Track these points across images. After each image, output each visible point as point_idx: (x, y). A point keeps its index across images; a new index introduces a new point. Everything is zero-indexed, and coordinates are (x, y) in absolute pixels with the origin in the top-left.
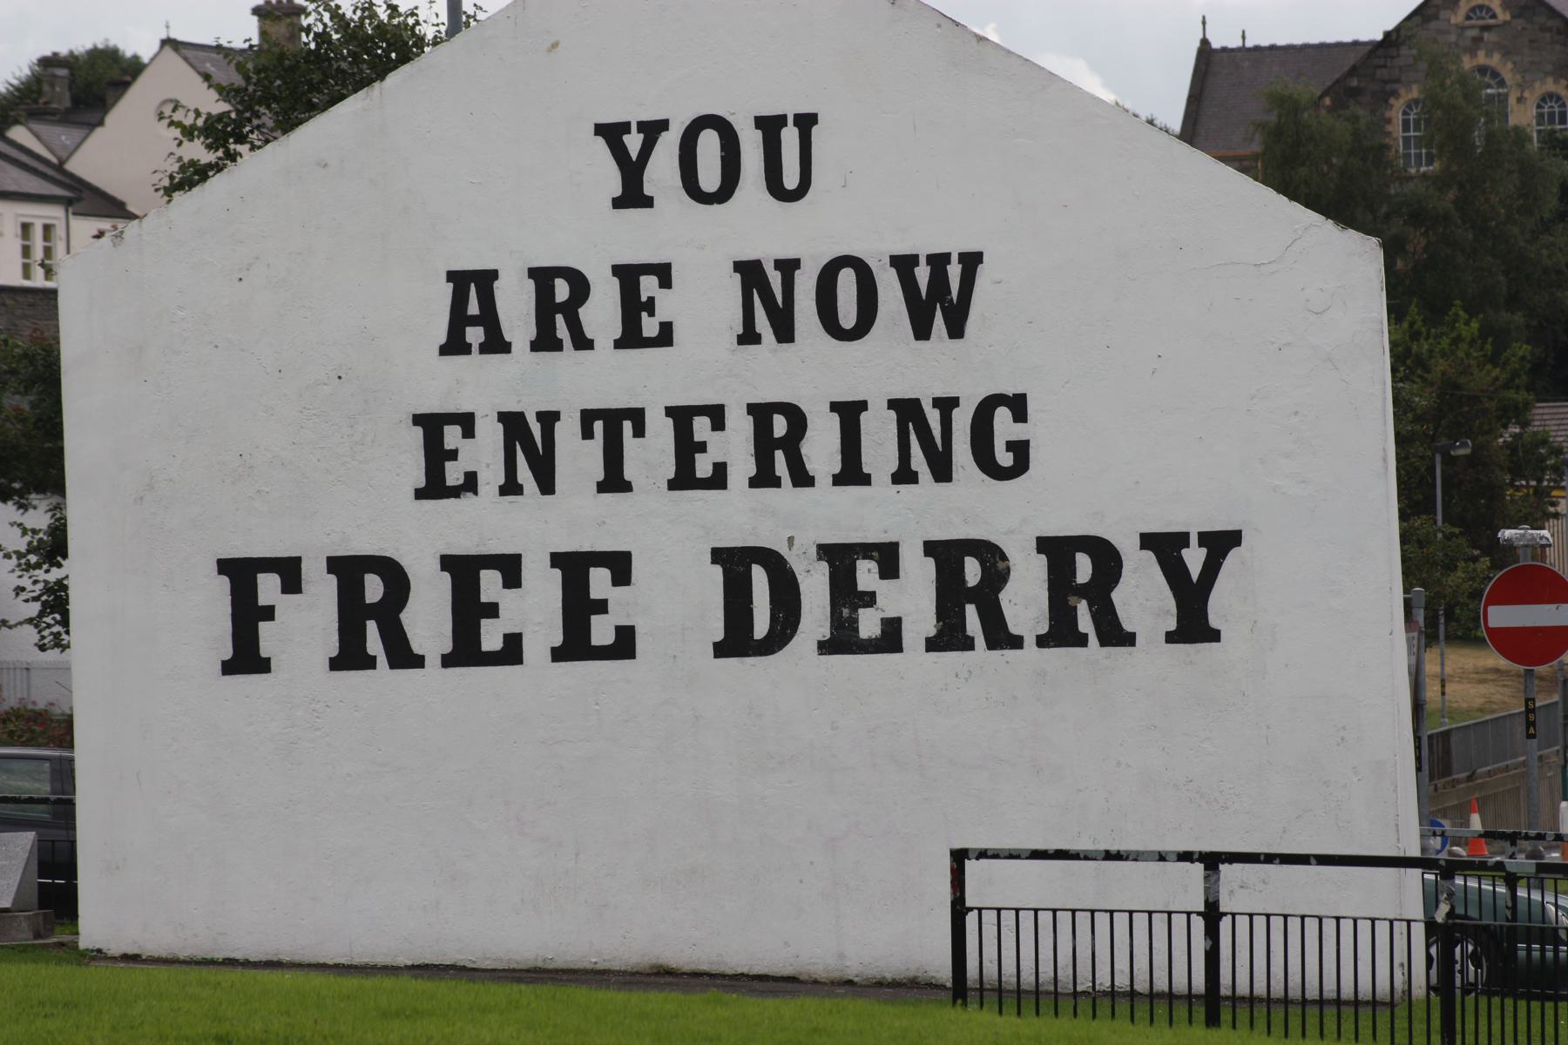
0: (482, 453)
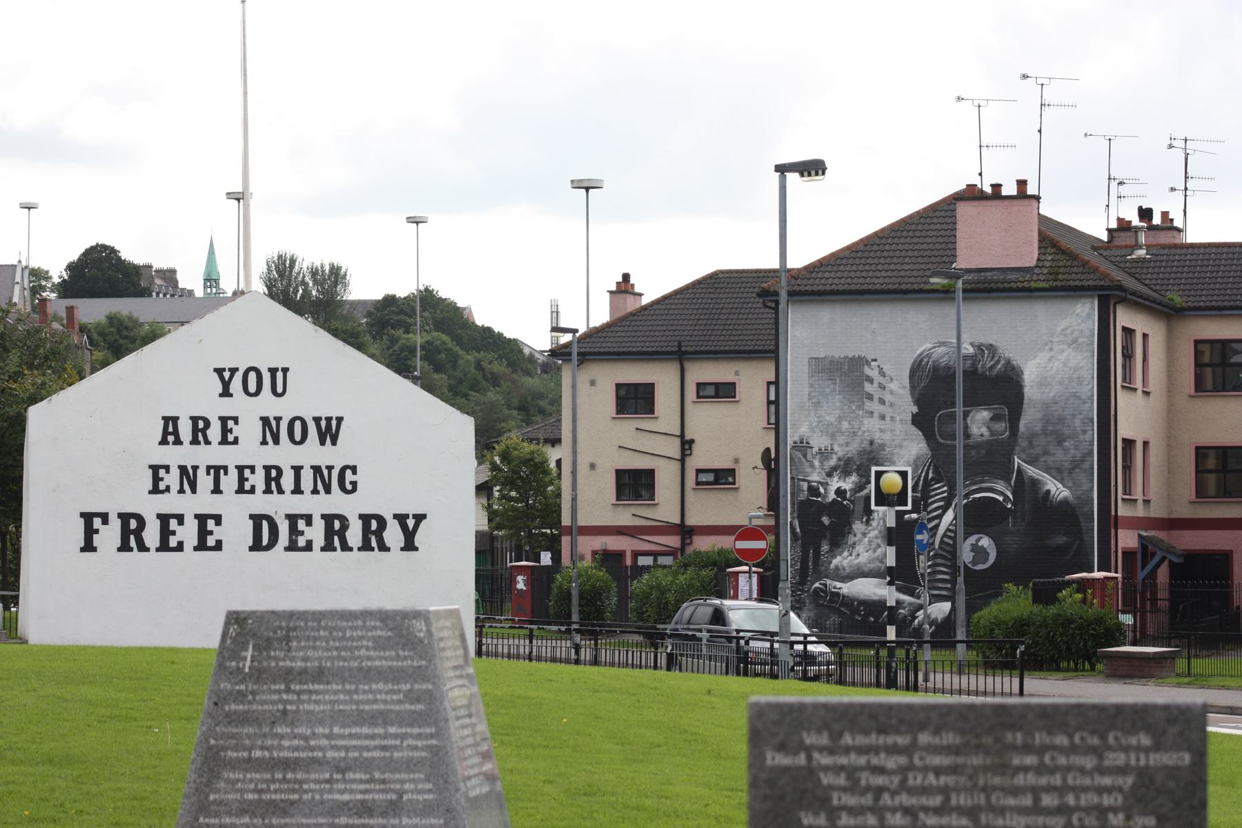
0: (172, 479)
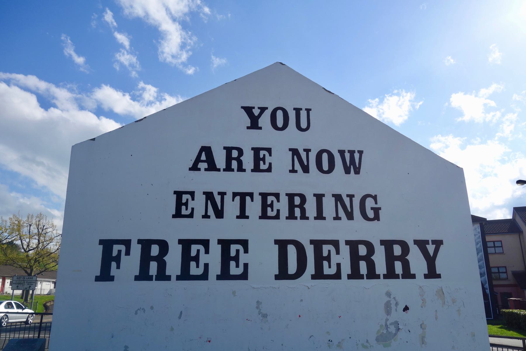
0: (199, 204)
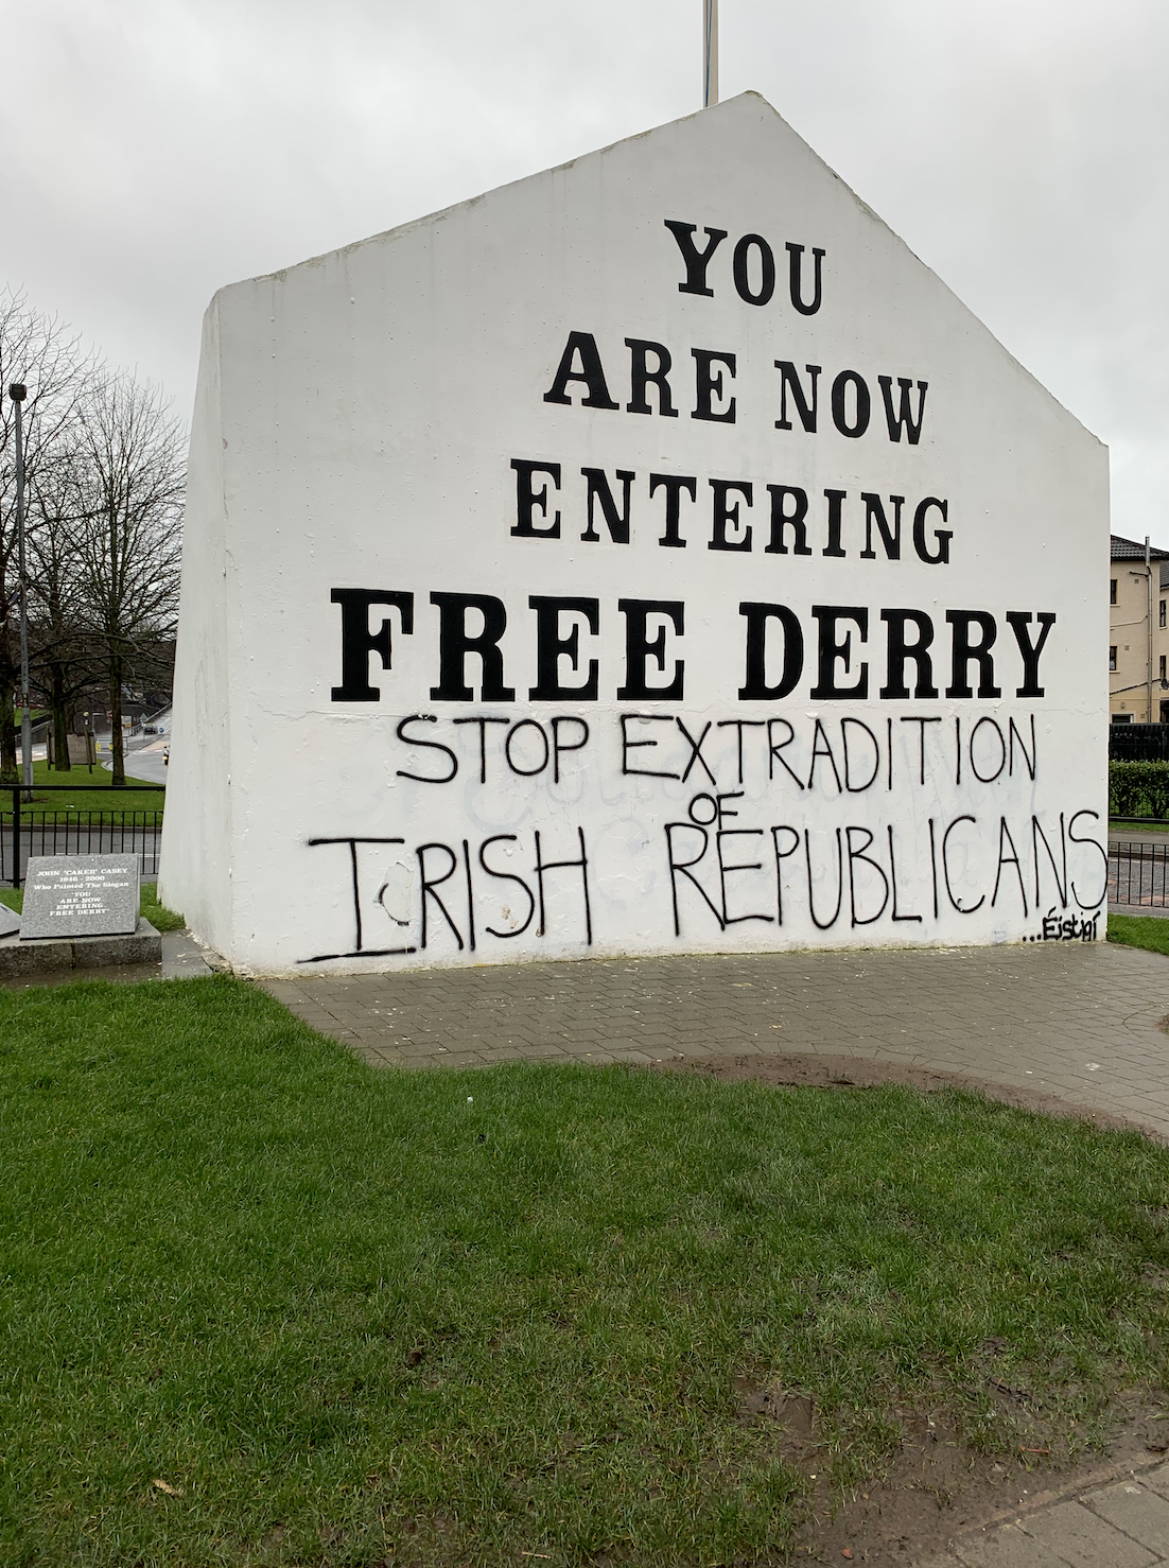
0: (569, 501)
